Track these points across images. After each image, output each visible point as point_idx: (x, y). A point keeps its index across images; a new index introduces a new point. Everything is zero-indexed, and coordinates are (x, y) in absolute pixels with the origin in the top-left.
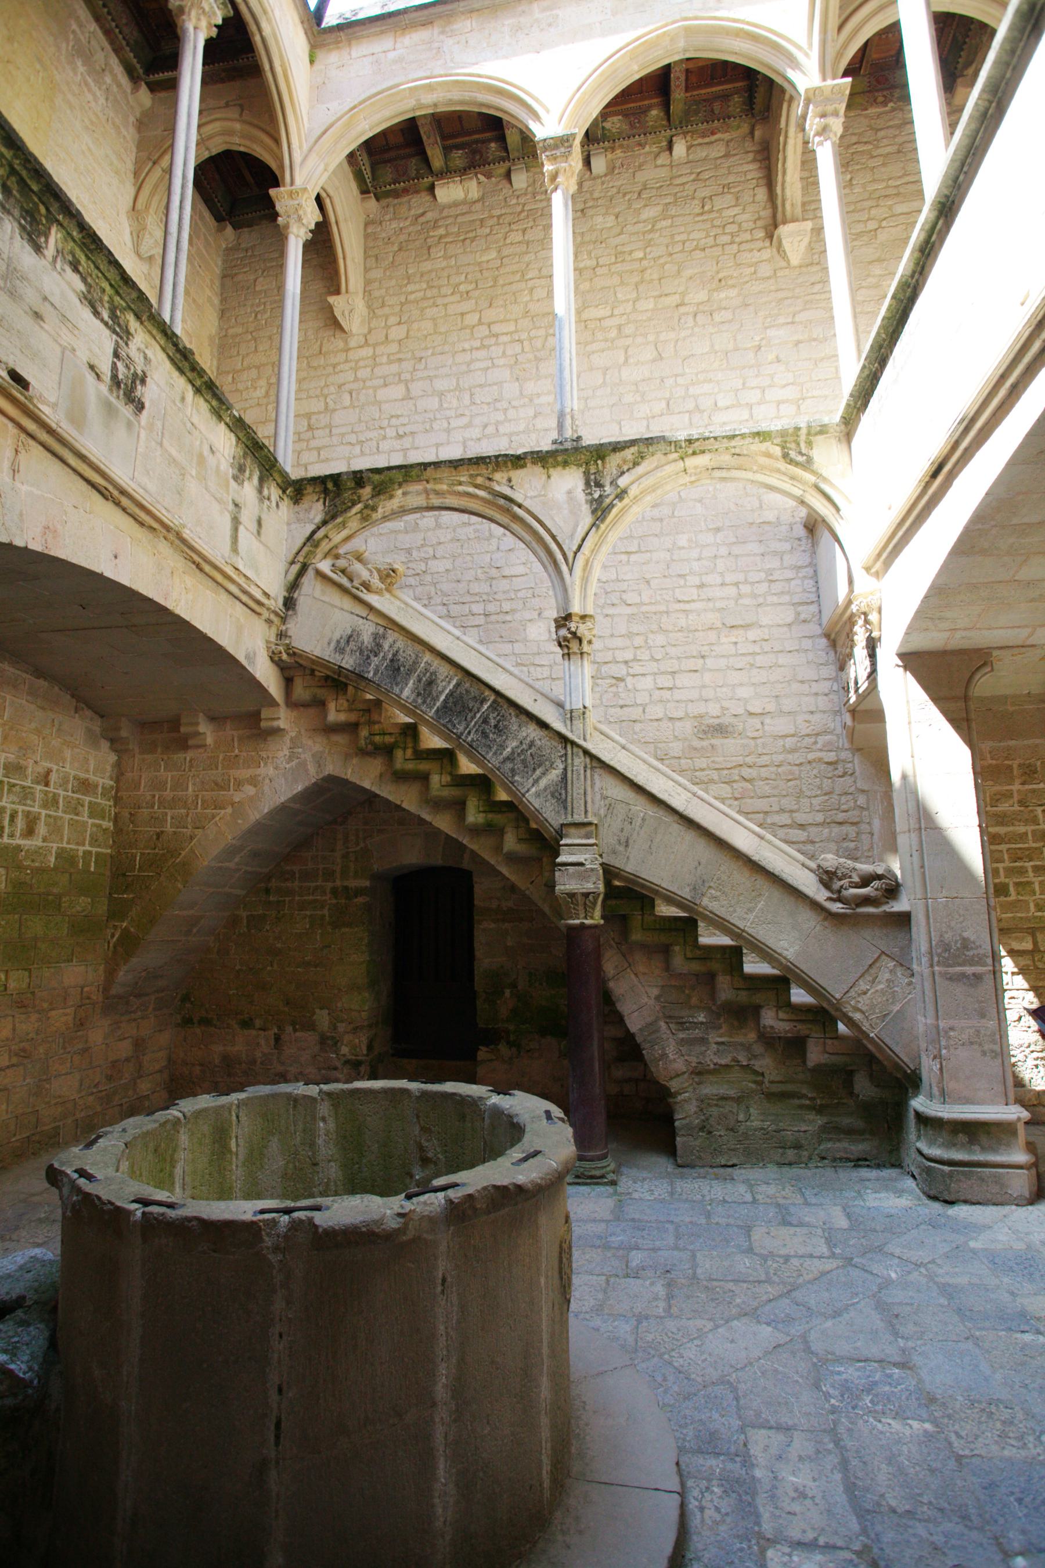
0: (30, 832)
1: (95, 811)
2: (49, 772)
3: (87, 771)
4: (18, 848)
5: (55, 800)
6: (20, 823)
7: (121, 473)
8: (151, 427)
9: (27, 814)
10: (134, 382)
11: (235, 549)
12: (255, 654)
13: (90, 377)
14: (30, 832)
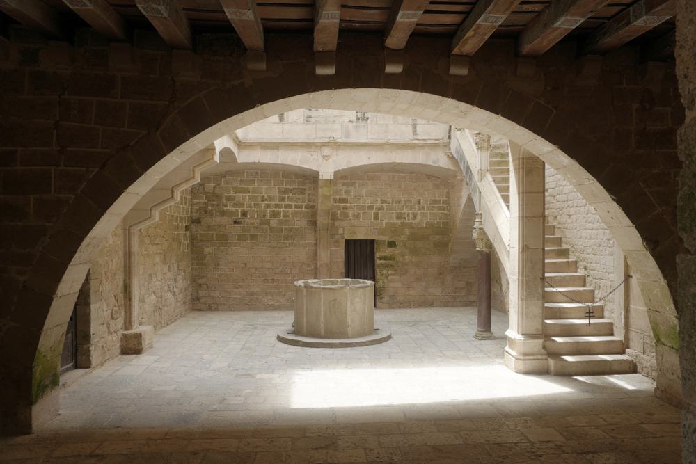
0: (415, 218)
1: (439, 209)
2: (420, 200)
3: (435, 197)
4: (412, 223)
5: (423, 208)
6: (411, 216)
7: (363, 139)
8: (372, 122)
9: (413, 213)
10: (364, 115)
11: (416, 134)
12: (438, 159)
13: (350, 125)
14: (415, 218)
